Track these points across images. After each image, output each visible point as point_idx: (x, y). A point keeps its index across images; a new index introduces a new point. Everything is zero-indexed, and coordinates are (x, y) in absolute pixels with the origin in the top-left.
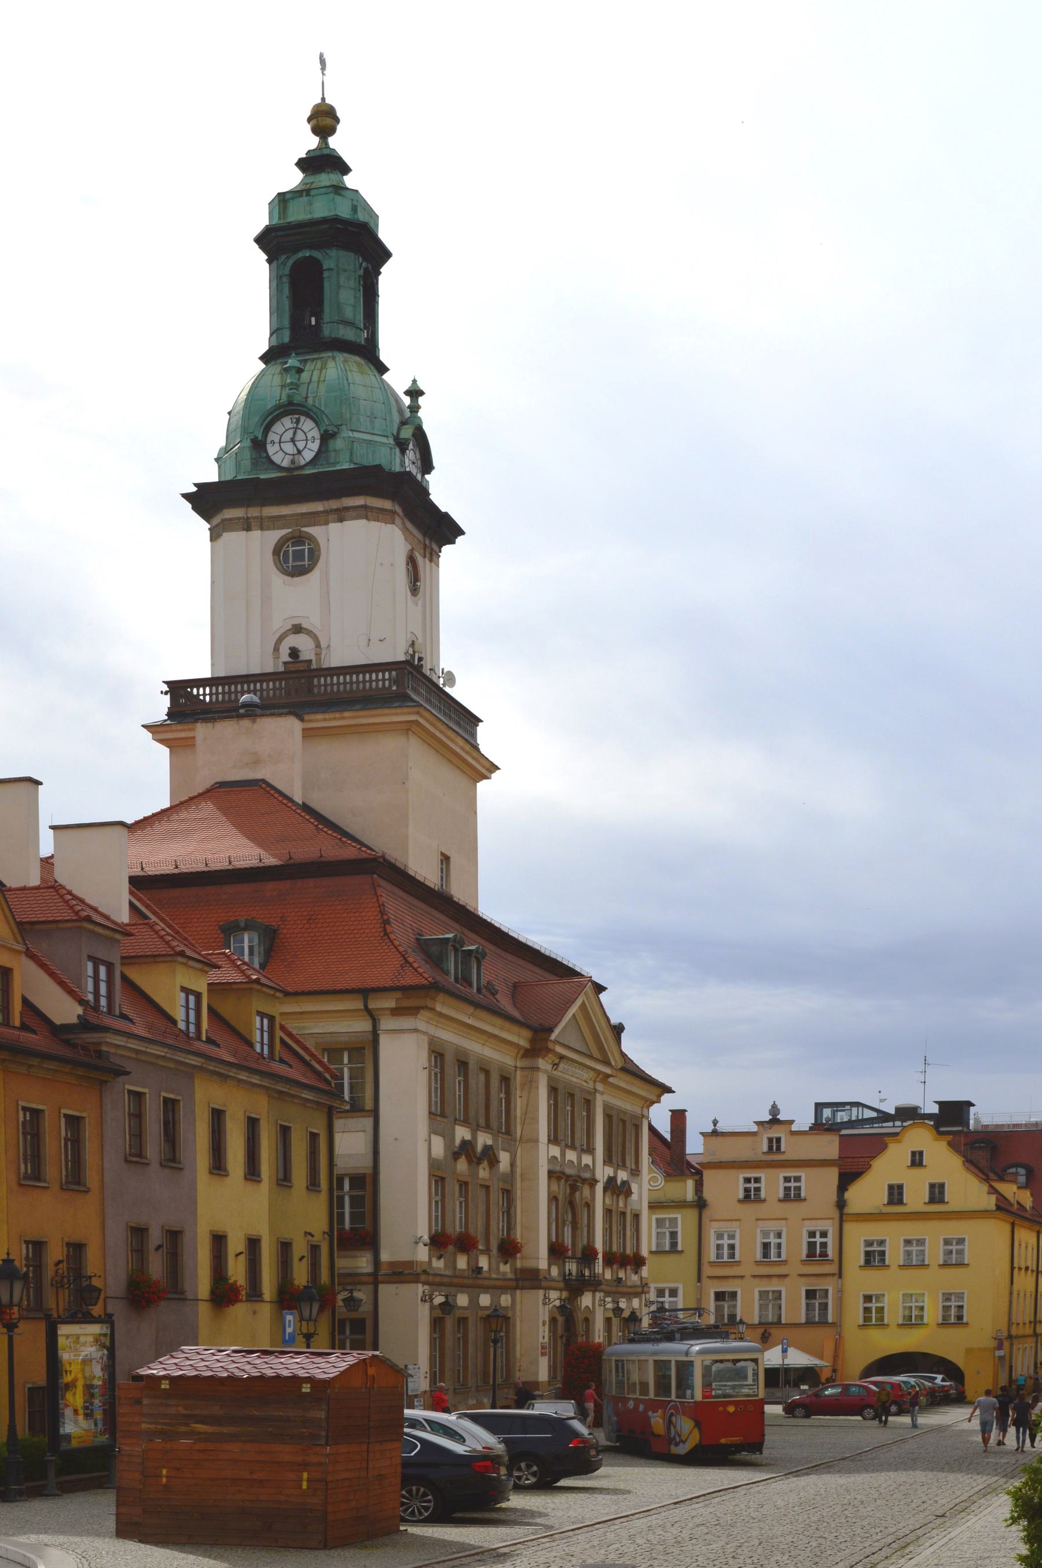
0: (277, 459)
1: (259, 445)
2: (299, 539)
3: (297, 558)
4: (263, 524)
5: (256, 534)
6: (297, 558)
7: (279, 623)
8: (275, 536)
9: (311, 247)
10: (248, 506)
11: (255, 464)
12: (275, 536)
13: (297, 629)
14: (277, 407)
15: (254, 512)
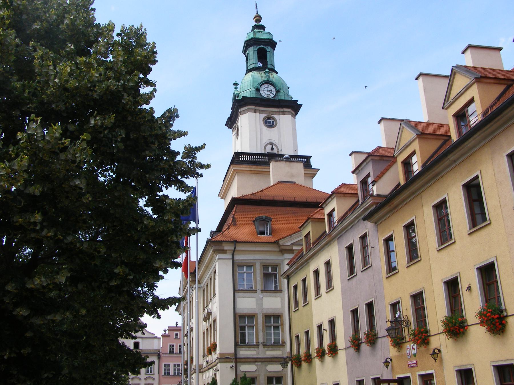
0: (263, 95)
1: (258, 90)
2: (269, 118)
3: (270, 122)
4: (261, 112)
5: (258, 114)
6: (270, 122)
7: (265, 141)
8: (263, 116)
9: (263, 45)
10: (256, 106)
11: (256, 94)
12: (263, 116)
13: (271, 143)
14: (261, 83)
15: (257, 108)
